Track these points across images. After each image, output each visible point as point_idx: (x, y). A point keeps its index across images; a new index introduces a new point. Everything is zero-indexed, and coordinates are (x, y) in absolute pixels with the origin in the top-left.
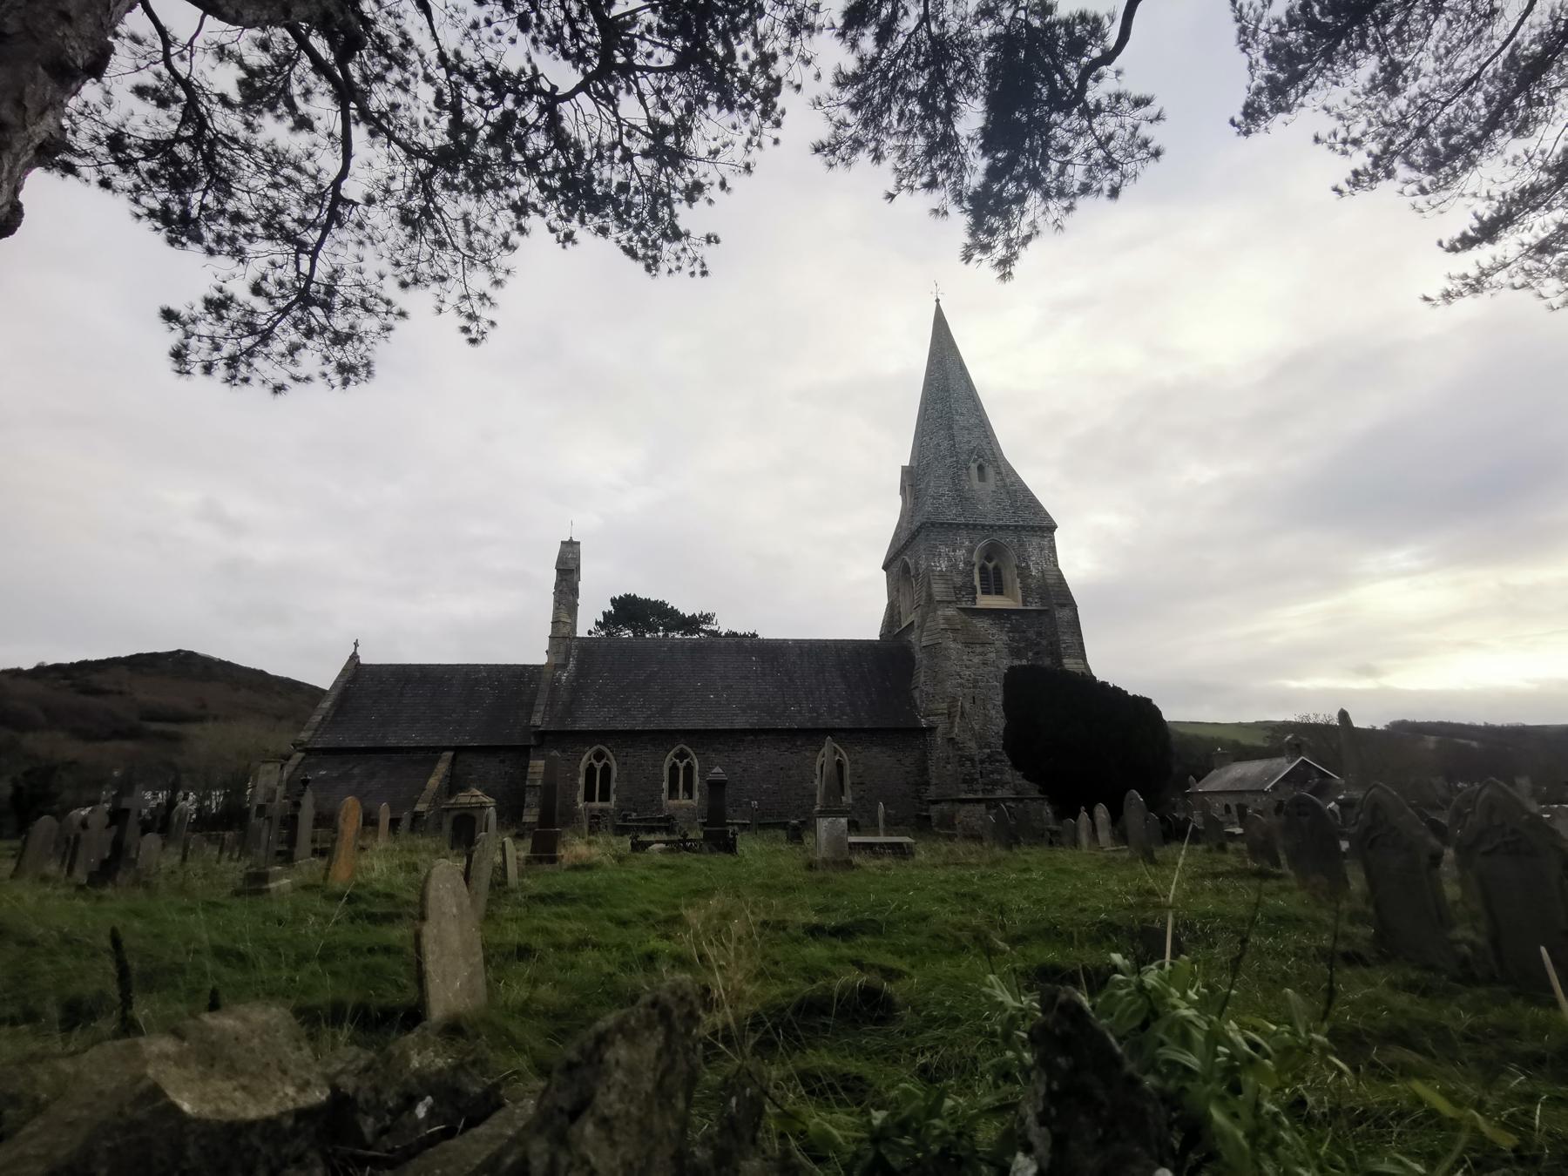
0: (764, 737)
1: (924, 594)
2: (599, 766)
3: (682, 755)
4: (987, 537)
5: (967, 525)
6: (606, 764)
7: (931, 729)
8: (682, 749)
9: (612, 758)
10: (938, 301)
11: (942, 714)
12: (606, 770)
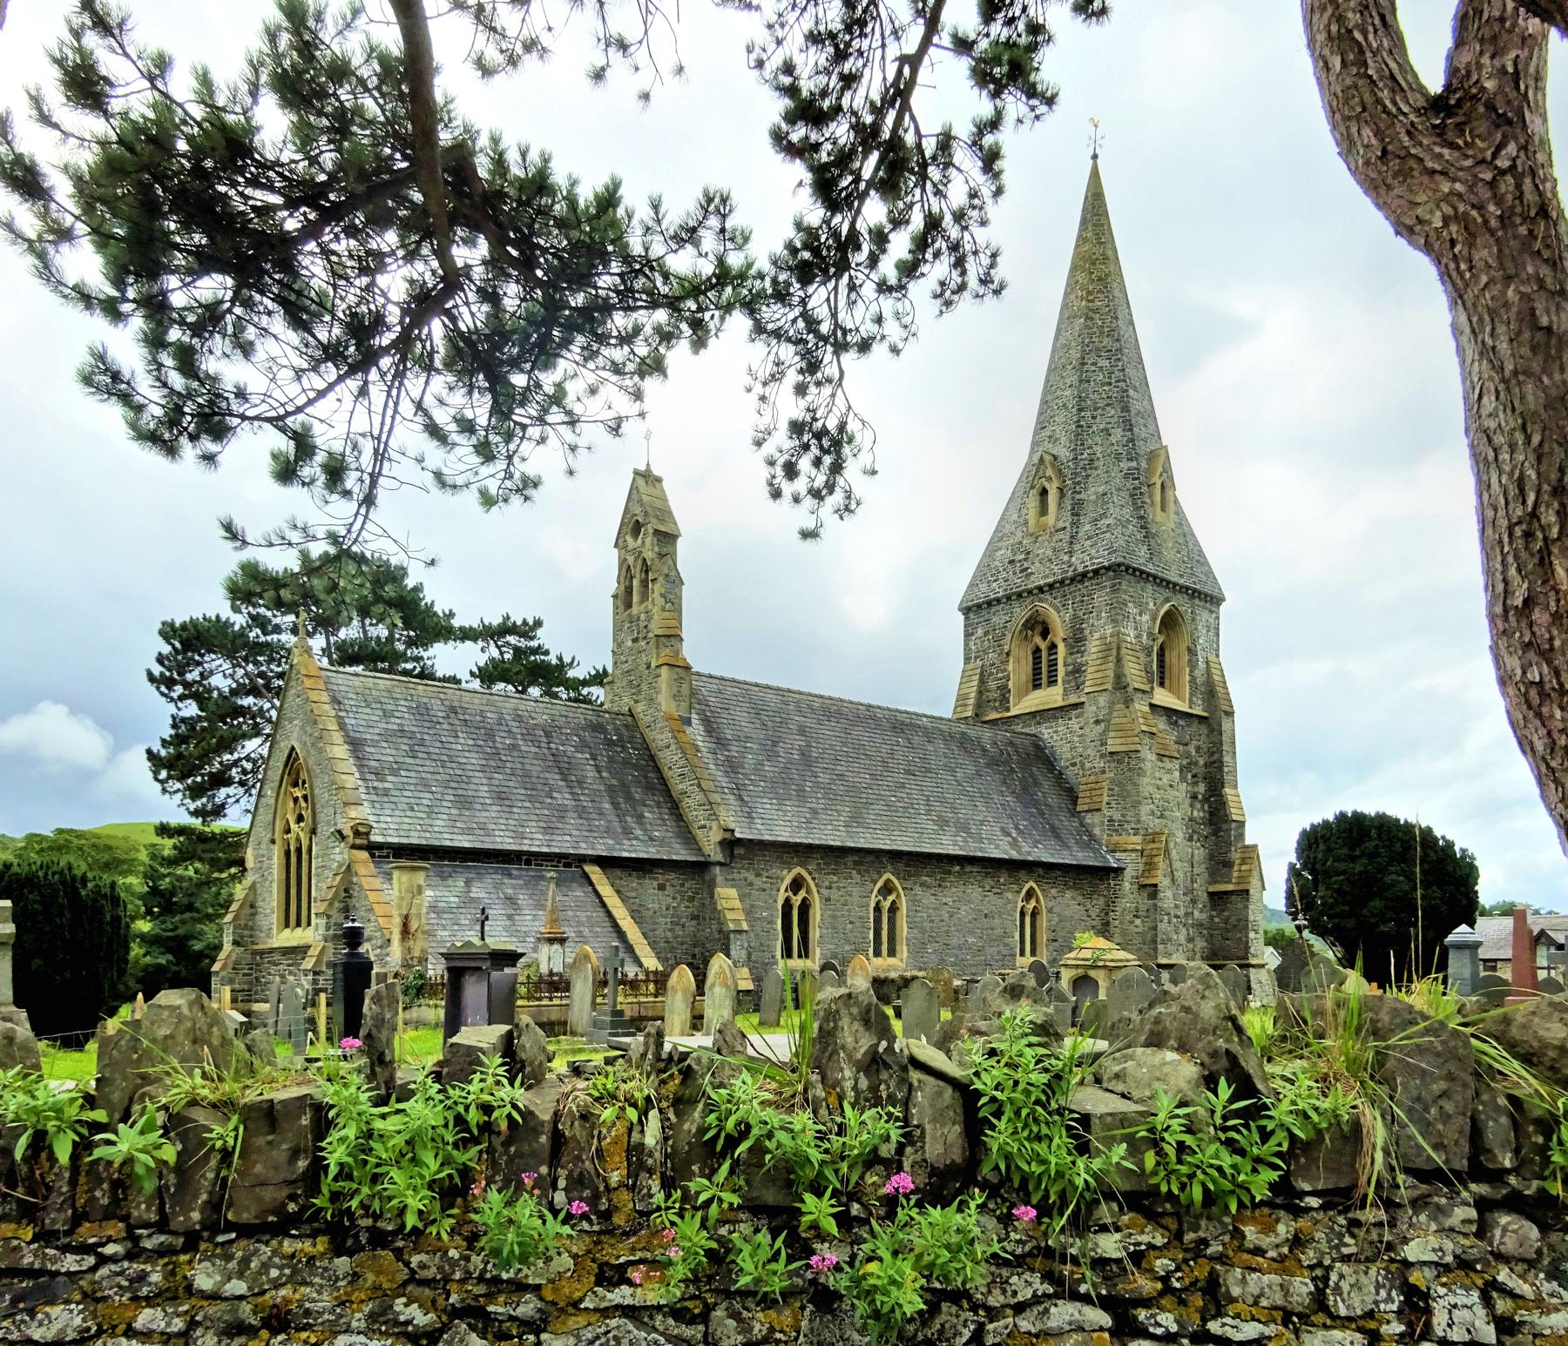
0: (968, 869)
1: (1111, 673)
2: (797, 901)
3: (887, 889)
4: (1167, 600)
5: (1155, 577)
6: (804, 900)
7: (1119, 871)
8: (889, 880)
9: (814, 889)
10: (1095, 157)
12: (805, 907)
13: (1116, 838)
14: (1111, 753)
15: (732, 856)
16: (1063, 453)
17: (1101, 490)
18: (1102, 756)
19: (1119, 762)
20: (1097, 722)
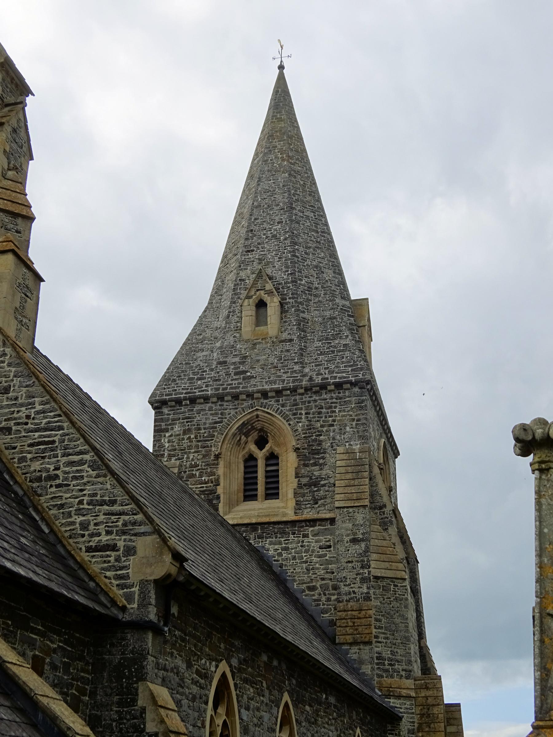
1: (367, 488)
10: (281, 67)
11: (409, 697)
13: (387, 681)
14: (376, 578)
15: (165, 615)
16: (281, 276)
17: (328, 314)
18: (364, 580)
19: (386, 589)
20: (355, 541)
